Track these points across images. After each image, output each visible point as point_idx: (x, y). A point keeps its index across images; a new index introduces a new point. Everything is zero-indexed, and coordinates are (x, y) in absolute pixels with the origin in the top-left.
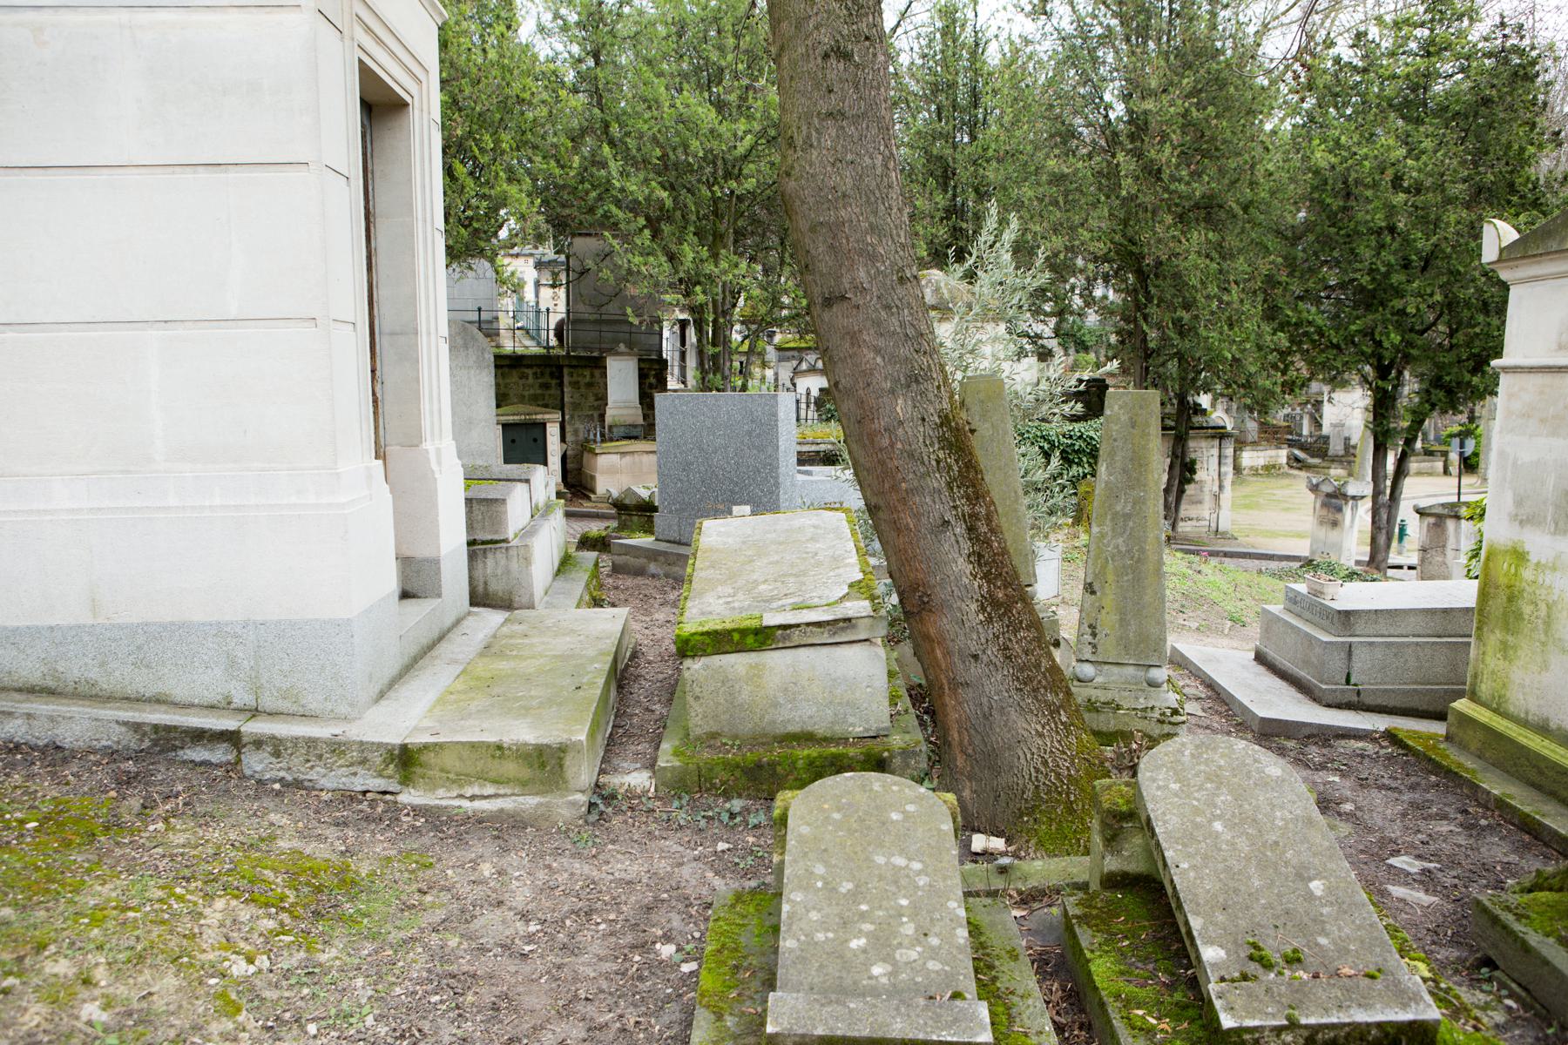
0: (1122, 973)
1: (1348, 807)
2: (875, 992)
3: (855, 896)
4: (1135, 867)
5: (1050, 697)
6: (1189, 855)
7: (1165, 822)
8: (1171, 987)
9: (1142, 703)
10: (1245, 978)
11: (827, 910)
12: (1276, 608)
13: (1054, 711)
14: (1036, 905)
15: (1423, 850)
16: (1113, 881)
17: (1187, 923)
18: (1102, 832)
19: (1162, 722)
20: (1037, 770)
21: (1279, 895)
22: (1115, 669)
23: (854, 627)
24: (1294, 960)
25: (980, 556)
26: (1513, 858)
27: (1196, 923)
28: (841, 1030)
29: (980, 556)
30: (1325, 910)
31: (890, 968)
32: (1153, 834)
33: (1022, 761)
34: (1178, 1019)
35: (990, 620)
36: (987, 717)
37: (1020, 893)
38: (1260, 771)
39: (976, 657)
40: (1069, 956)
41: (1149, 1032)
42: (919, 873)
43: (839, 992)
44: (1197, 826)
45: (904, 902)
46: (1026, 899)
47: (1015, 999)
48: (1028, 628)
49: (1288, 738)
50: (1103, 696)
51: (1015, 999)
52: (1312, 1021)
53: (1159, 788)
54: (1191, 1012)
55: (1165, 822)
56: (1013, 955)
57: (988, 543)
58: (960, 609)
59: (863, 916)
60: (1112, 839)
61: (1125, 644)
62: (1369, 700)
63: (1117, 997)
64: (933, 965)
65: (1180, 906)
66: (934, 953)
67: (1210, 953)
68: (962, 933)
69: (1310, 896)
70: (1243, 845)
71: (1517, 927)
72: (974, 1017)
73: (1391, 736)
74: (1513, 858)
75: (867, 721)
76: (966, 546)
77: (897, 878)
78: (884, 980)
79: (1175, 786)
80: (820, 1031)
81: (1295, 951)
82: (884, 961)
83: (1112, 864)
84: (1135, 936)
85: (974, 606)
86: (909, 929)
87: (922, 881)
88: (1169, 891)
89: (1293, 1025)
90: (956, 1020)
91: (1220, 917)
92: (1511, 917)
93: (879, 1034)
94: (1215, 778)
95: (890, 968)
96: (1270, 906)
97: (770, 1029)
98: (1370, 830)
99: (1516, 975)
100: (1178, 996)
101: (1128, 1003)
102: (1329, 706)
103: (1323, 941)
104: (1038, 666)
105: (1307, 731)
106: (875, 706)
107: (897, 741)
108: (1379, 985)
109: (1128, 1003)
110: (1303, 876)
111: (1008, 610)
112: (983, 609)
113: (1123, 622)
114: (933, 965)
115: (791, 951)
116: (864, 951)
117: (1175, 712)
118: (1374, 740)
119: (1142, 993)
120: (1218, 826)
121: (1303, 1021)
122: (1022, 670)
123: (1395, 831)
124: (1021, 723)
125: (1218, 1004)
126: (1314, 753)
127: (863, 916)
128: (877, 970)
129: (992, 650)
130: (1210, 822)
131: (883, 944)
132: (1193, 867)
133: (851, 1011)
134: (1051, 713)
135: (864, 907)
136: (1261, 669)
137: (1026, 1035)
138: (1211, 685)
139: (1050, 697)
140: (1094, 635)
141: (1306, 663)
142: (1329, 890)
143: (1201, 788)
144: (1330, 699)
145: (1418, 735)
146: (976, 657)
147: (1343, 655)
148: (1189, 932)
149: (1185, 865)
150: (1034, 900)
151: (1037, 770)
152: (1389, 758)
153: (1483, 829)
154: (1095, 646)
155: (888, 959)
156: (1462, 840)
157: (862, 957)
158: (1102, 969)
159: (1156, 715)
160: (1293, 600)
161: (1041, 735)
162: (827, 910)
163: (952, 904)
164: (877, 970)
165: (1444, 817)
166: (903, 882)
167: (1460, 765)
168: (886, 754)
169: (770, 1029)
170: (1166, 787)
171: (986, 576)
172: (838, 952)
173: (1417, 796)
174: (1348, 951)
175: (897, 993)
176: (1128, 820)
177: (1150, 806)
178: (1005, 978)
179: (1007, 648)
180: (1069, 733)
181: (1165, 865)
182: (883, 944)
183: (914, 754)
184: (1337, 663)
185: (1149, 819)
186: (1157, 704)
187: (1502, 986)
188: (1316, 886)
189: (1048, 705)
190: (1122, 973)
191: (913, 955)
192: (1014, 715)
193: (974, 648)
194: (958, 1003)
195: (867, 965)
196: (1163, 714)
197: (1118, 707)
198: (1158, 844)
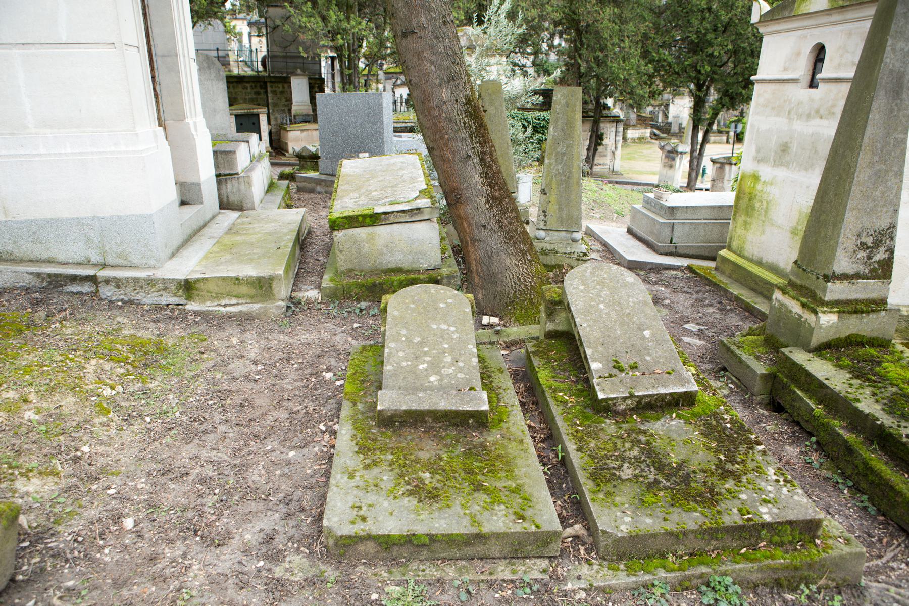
0: (553, 377)
1: (667, 302)
2: (431, 389)
3: (421, 344)
4: (561, 328)
5: (522, 247)
6: (587, 320)
8: (576, 383)
9: (569, 250)
10: (611, 376)
11: (407, 351)
12: (639, 206)
13: (524, 254)
14: (513, 349)
15: (700, 321)
16: (550, 335)
17: (585, 352)
18: (546, 311)
20: (515, 284)
21: (629, 338)
22: (556, 233)
23: (422, 212)
24: (634, 367)
25: (487, 174)
26: (740, 323)
27: (589, 352)
28: (415, 407)
29: (487, 174)
30: (650, 344)
31: (439, 377)
32: (570, 311)
34: (578, 397)
37: (505, 343)
38: (623, 280)
40: (529, 371)
41: (565, 403)
42: (454, 332)
43: (414, 389)
44: (592, 306)
45: (446, 346)
46: (509, 346)
47: (501, 391)
48: (511, 211)
49: (641, 270)
51: (501, 391)
52: (640, 394)
54: (585, 393)
56: (501, 371)
59: (425, 353)
60: (551, 315)
61: (561, 220)
62: (680, 251)
63: (550, 388)
64: (460, 375)
65: (582, 344)
66: (461, 370)
67: (595, 366)
68: (475, 360)
69: (643, 338)
70: (613, 315)
71: (738, 352)
72: (480, 398)
73: (690, 268)
74: (740, 323)
77: (443, 335)
78: (436, 383)
79: (582, 288)
80: (404, 408)
81: (635, 363)
82: (436, 374)
83: (550, 326)
84: (560, 360)
85: (483, 200)
86: (449, 359)
87: (455, 336)
88: (577, 337)
89: (631, 396)
90: (471, 400)
91: (601, 349)
92: (736, 348)
93: (433, 408)
94: (602, 283)
95: (439, 377)
96: (625, 343)
97: (379, 408)
98: (676, 312)
99: (735, 374)
100: (579, 386)
101: (555, 390)
102: (661, 254)
103: (648, 358)
104: (516, 231)
105: (650, 266)
108: (672, 377)
109: (555, 390)
110: (641, 329)
111: (501, 202)
112: (488, 201)
114: (460, 375)
115: (389, 371)
116: (426, 370)
117: (585, 254)
118: (682, 270)
119: (562, 386)
120: (602, 306)
121: (636, 394)
122: (508, 233)
123: (688, 313)
124: (507, 260)
125: (597, 388)
126: (653, 277)
127: (425, 353)
128: (432, 379)
129: (493, 223)
130: (598, 304)
131: (435, 367)
132: (589, 326)
133: (419, 398)
135: (426, 349)
136: (630, 237)
137: (506, 406)
138: (605, 245)
139: (522, 247)
140: (545, 216)
141: (652, 233)
142: (653, 335)
143: (594, 288)
144: (662, 250)
145: (702, 268)
146: (484, 226)
147: (670, 229)
148: (586, 357)
149: (584, 325)
150: (512, 346)
151: (515, 284)
152: (688, 278)
153: (728, 310)
155: (438, 373)
156: (718, 316)
157: (425, 373)
158: (544, 376)
159: (576, 256)
160: (647, 202)
161: (517, 266)
162: (407, 351)
163: (470, 347)
164: (432, 379)
165: (711, 305)
166: (446, 336)
167: (720, 281)
169: (379, 408)
171: (490, 185)
172: (413, 371)
173: (699, 296)
174: (659, 362)
175: (442, 389)
176: (559, 305)
177: (569, 297)
179: (500, 222)
180: (531, 265)
181: (575, 325)
182: (435, 367)
183: (454, 277)
184: (666, 233)
185: (568, 304)
187: (729, 378)
188: (647, 333)
189: (521, 251)
190: (553, 377)
191: (451, 371)
192: (503, 256)
193: (483, 222)
194: (472, 392)
195: (428, 376)
197: (557, 252)
198: (572, 316)
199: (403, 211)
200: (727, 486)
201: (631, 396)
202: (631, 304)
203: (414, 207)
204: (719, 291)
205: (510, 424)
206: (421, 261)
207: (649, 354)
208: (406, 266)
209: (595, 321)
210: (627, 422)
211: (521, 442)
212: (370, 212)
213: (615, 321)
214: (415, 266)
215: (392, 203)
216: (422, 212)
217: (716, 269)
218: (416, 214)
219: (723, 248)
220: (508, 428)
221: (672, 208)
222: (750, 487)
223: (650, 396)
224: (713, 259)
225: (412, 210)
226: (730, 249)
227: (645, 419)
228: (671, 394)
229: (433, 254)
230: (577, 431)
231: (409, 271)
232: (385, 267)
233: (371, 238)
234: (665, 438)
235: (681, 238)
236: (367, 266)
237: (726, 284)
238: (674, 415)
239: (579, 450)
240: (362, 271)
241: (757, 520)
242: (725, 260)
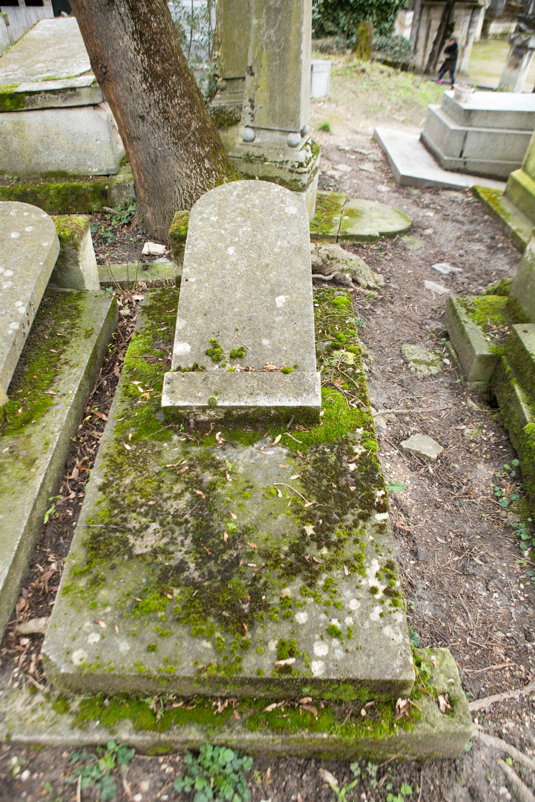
1: (429, 231)
5: (197, 150)
7: (194, 246)
9: (281, 158)
10: (195, 368)
12: (435, 107)
13: (200, 160)
15: (458, 260)
19: (291, 171)
20: (186, 201)
21: (251, 306)
22: (268, 134)
23: (79, 94)
24: (237, 356)
25: (142, 34)
26: (506, 268)
29: (142, 34)
30: (277, 319)
33: (177, 194)
35: (151, 88)
36: (154, 162)
38: (281, 209)
39: (142, 118)
44: (216, 249)
48: (182, 96)
49: (416, 188)
50: (257, 152)
52: (226, 404)
53: (202, 219)
55: (194, 246)
57: (147, 22)
58: (128, 79)
61: (272, 115)
62: (470, 168)
67: (180, 348)
69: (273, 307)
70: (242, 267)
71: (464, 318)
73: (474, 191)
74: (506, 268)
75: (100, 164)
76: (130, 24)
79: (214, 219)
81: (242, 349)
85: (139, 77)
89: (212, 406)
91: (200, 321)
92: (464, 311)
94: (246, 214)
96: (240, 314)
98: (434, 246)
99: (455, 345)
102: (446, 170)
103: (265, 342)
104: (188, 126)
105: (427, 185)
106: (103, 154)
107: (120, 178)
108: (287, 378)
110: (274, 293)
111: (165, 81)
112: (145, 80)
113: (272, 98)
117: (301, 165)
118: (465, 192)
120: (231, 251)
121: (220, 404)
122: (176, 129)
123: (447, 249)
124: (177, 168)
126: (427, 198)
129: (154, 114)
130: (227, 247)
132: (199, 282)
134: (198, 161)
136: (420, 146)
138: (385, 154)
139: (197, 150)
140: (253, 107)
141: (441, 143)
142: (288, 303)
143: (233, 220)
144: (448, 166)
145: (488, 191)
146: (142, 118)
147: (461, 138)
151: (186, 201)
152: (468, 203)
153: (498, 249)
154: (253, 116)
156: (483, 256)
159: (289, 166)
160: (446, 101)
161: (189, 177)
165: (480, 240)
167: (502, 210)
168: (107, 187)
170: (208, 219)
171: (147, 52)
173: (471, 227)
174: (280, 350)
178: (70, 351)
179: (165, 112)
180: (210, 176)
183: (126, 188)
184: (456, 144)
186: (290, 159)
187: (448, 351)
188: (280, 300)
189: (195, 155)
192: (172, 162)
193: (140, 110)
196: (293, 166)
197: (265, 160)
199: (53, 92)
200: (287, 592)
201: (212, 406)
202: (277, 250)
203: (68, 85)
204: (498, 223)
205: (38, 428)
206: (89, 163)
207: (269, 336)
208: (70, 169)
209: (211, 274)
210: (202, 443)
211: (32, 462)
212: (9, 90)
213: (241, 277)
214: (82, 170)
215: (47, 80)
216: (79, 94)
217: (505, 194)
218: (71, 96)
219: (518, 167)
220: (29, 436)
221: (469, 112)
222: (325, 597)
223: (242, 408)
224: (504, 179)
225: (64, 90)
226: (525, 169)
227: (232, 441)
228: (276, 408)
229: (103, 154)
230: (121, 453)
231: (75, 177)
232: (44, 170)
233: (19, 128)
234: (242, 480)
235: (474, 152)
236: (21, 168)
237: (508, 215)
238: (278, 438)
239: (103, 488)
240: (16, 173)
241: (301, 673)
242: (516, 184)
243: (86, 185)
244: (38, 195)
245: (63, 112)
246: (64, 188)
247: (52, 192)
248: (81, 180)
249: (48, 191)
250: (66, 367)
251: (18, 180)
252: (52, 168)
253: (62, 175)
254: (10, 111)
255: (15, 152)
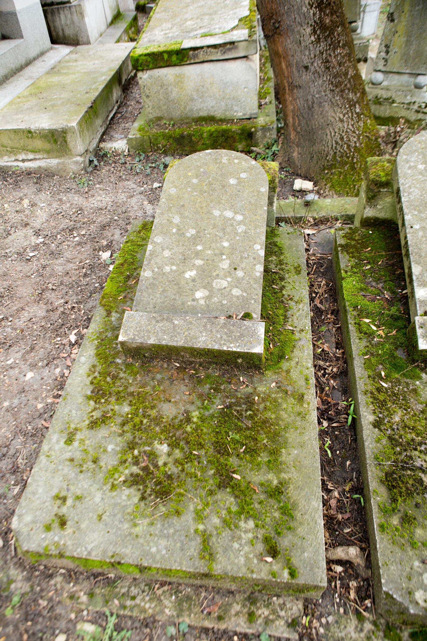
0: (362, 289)
5: (351, 96)
7: (410, 193)
9: (409, 99)
13: (352, 105)
19: (418, 112)
20: (337, 143)
22: (396, 77)
33: (329, 137)
35: (318, 40)
36: (310, 108)
39: (306, 68)
50: (385, 94)
53: (410, 168)
55: (410, 193)
58: (299, 32)
65: (408, 255)
75: (245, 109)
104: (346, 74)
106: (249, 100)
107: (261, 121)
113: (408, 43)
122: (335, 77)
124: (331, 113)
129: (318, 63)
134: (350, 106)
139: (351, 96)
146: (306, 68)
151: (337, 143)
154: (386, 60)
158: (350, 285)
159: (416, 107)
161: (342, 121)
168: (253, 130)
170: (415, 167)
178: (289, 287)
179: (327, 61)
180: (359, 119)
183: (269, 130)
186: (418, 100)
189: (349, 101)
190: (362, 289)
193: (306, 61)
196: (420, 107)
197: (393, 102)
199: (214, 46)
203: (228, 40)
205: (293, 363)
206: (235, 108)
208: (218, 114)
211: (301, 398)
212: (176, 47)
214: (228, 115)
215: (205, 35)
216: (236, 48)
218: (230, 50)
220: (288, 372)
225: (225, 44)
229: (249, 100)
230: (379, 390)
231: (222, 121)
232: (196, 115)
233: (180, 79)
236: (177, 114)
239: (377, 424)
240: (171, 119)
243: (234, 128)
244: (193, 138)
245: (219, 64)
246: (216, 131)
247: (205, 135)
248: (228, 123)
249: (202, 135)
250: (292, 303)
251: (173, 125)
252: (203, 114)
253: (211, 119)
254: (175, 65)
255: (173, 100)
